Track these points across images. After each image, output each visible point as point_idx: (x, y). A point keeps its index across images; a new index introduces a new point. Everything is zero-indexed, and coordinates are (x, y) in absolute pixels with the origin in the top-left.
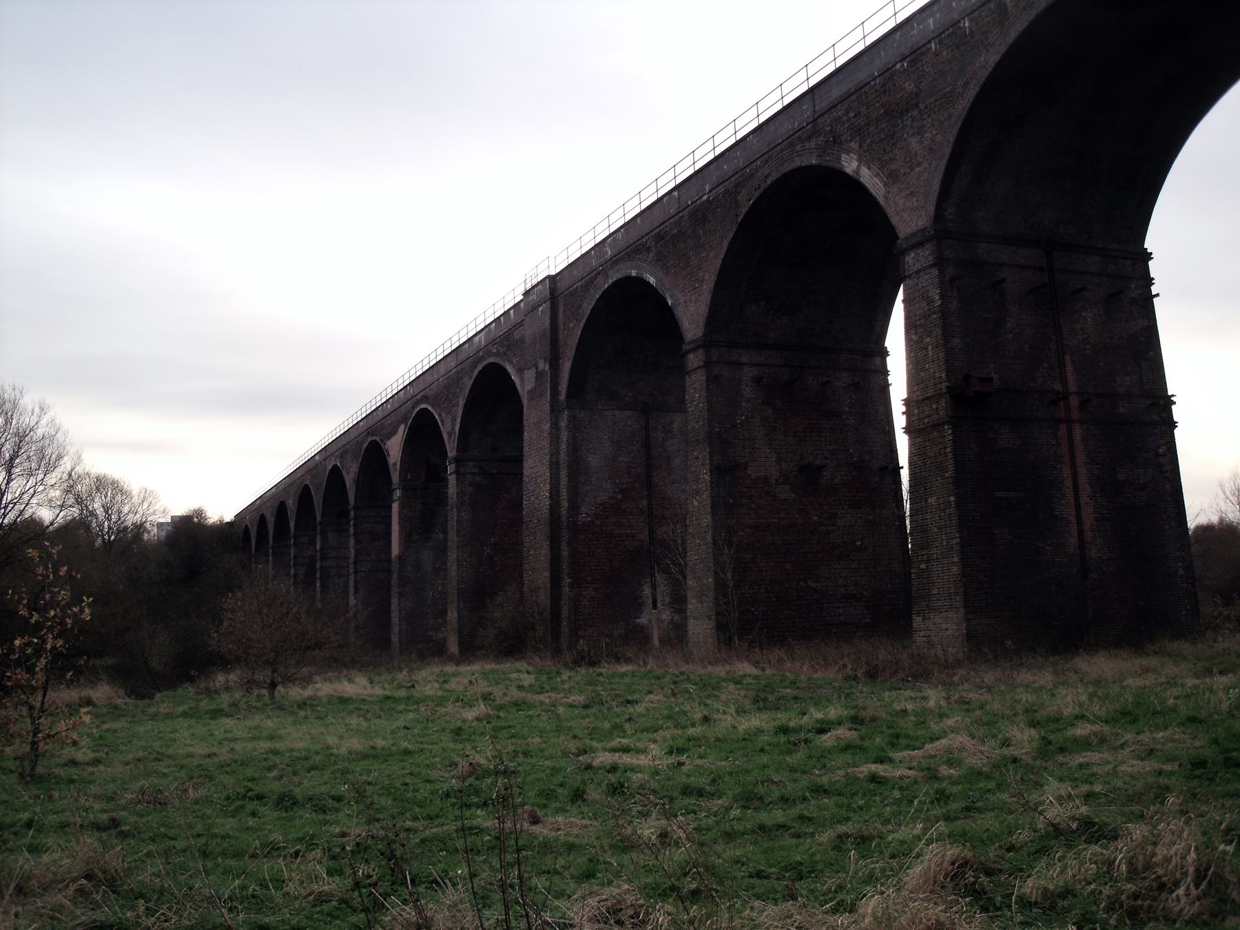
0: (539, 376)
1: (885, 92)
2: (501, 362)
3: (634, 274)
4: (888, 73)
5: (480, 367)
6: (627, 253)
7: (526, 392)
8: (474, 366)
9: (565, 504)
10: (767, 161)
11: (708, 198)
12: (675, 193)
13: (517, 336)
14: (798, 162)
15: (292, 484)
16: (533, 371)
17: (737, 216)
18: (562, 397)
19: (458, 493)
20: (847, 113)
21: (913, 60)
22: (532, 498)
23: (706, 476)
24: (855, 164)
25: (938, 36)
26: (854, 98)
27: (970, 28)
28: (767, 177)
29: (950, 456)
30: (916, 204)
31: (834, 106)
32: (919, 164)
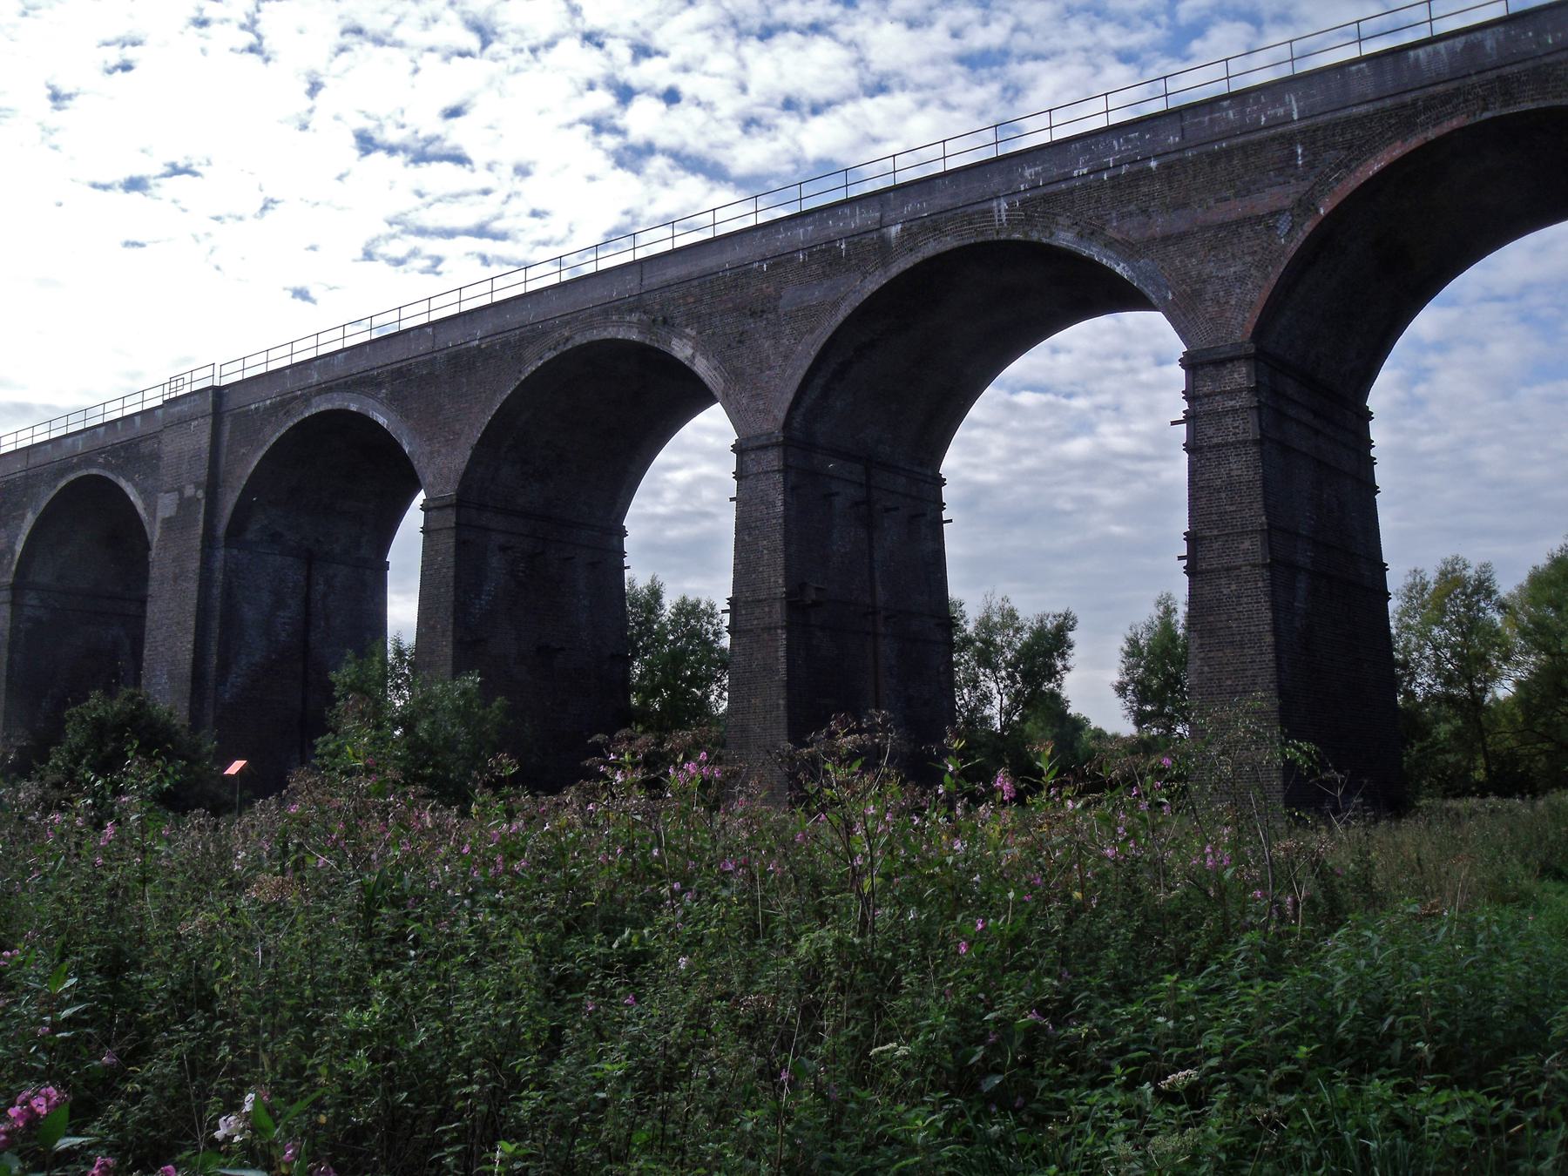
0: (185, 504)
1: (736, 286)
2: (111, 476)
3: (354, 408)
4: (743, 272)
5: (72, 477)
6: (346, 383)
7: (159, 520)
8: (61, 473)
9: (214, 660)
10: (569, 323)
11: (479, 346)
12: (429, 330)
13: (145, 448)
14: (610, 333)
15: (534, 334)
16: (174, 496)
17: (520, 372)
18: (221, 531)
19: (11, 629)
20: (684, 297)
21: (775, 264)
22: (161, 649)
23: (449, 651)
24: (689, 352)
25: (808, 249)
26: (695, 283)
27: (847, 250)
28: (567, 340)
29: (783, 660)
30: (762, 407)
31: (669, 286)
32: (771, 368)
